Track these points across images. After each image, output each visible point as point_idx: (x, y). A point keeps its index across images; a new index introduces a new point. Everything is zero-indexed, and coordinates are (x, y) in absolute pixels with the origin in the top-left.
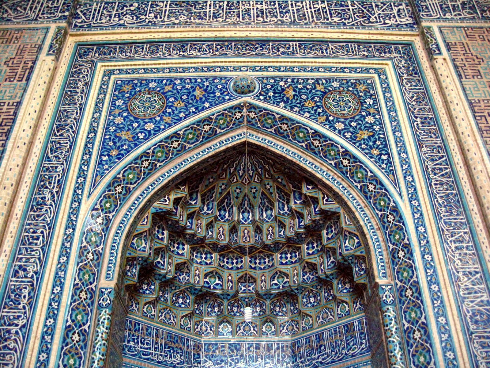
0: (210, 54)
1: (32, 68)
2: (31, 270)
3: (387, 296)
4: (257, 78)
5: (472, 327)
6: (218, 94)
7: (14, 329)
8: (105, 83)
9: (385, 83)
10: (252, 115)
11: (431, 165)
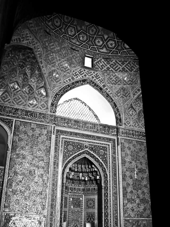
0: (81, 137)
1: (51, 137)
2: (55, 180)
3: (103, 188)
4: (89, 144)
5: (114, 194)
6: (82, 147)
7: (54, 190)
8: (62, 141)
9: (109, 148)
10: (87, 152)
11: (113, 167)
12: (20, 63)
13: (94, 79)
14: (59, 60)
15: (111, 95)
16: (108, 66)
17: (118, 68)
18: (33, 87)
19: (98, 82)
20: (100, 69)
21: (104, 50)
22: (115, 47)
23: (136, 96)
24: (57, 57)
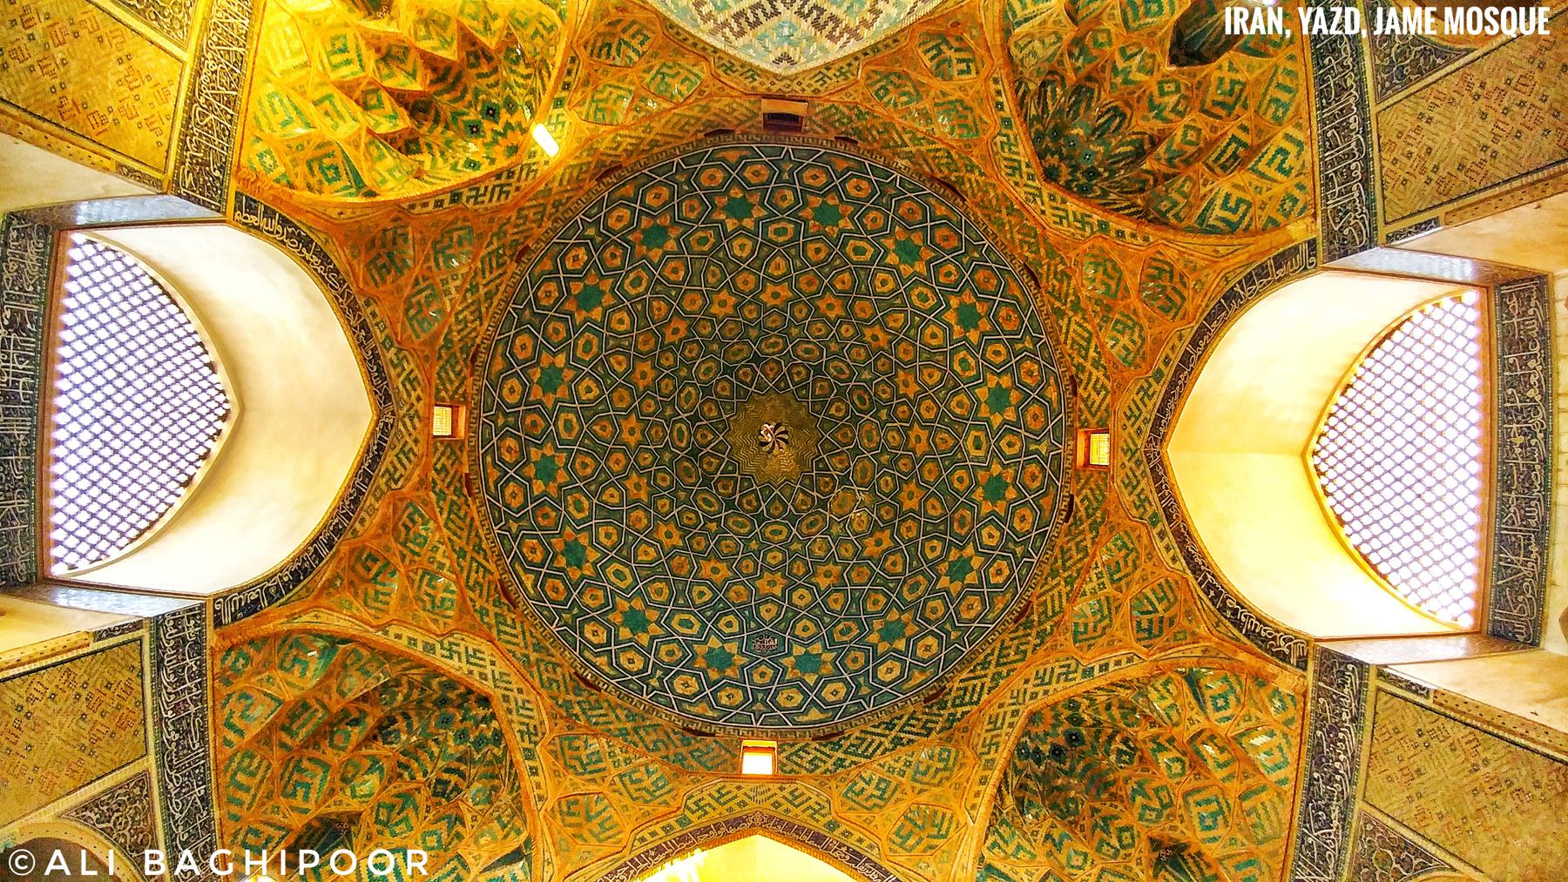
12: (446, 776)
13: (781, 809)
14: (627, 761)
15: (873, 855)
16: (840, 755)
17: (874, 746)
18: (469, 860)
19: (804, 816)
20: (804, 772)
21: (815, 714)
22: (847, 694)
23: (982, 809)
24: (618, 751)
